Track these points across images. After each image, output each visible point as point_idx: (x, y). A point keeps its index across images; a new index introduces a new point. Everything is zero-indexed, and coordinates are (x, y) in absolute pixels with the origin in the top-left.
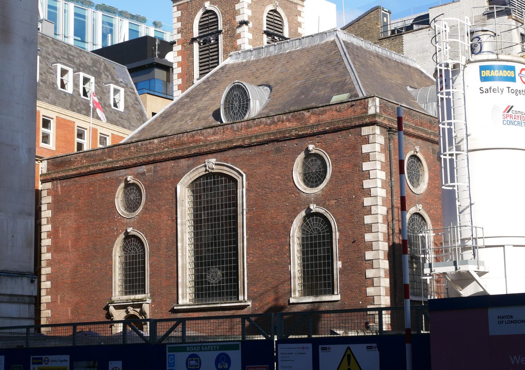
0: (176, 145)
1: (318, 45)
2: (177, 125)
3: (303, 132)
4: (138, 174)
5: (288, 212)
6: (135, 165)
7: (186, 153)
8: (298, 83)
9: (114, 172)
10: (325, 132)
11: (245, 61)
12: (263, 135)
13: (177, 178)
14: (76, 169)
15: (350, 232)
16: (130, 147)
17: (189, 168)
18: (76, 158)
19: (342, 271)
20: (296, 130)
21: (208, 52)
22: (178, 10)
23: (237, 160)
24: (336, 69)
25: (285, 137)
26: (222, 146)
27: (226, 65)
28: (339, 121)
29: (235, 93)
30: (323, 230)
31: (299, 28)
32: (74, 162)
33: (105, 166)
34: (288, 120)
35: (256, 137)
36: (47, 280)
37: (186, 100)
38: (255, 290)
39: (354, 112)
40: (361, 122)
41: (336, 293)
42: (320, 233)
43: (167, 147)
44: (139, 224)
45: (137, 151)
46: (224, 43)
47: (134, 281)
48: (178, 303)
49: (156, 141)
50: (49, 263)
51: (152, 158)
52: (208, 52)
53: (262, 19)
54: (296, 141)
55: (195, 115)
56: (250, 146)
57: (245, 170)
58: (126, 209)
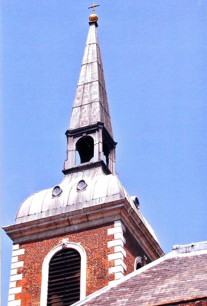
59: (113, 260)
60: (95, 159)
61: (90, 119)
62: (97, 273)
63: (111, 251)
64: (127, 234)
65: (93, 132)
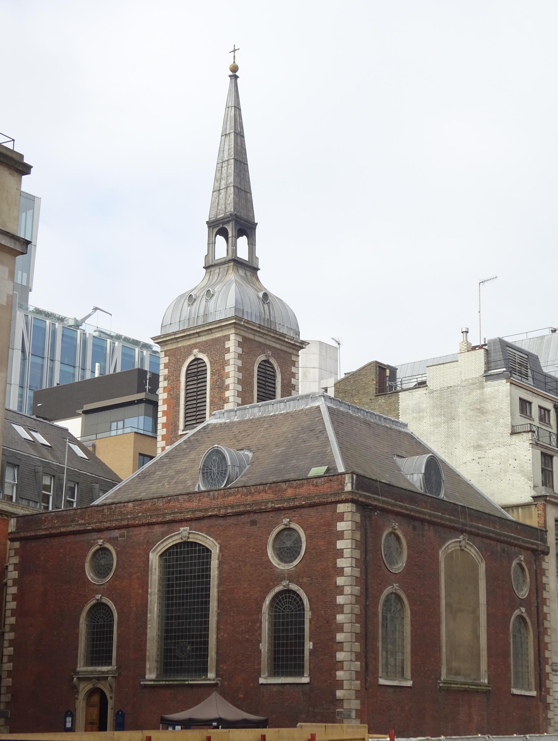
0: (150, 510)
1: (302, 410)
2: (154, 487)
3: (279, 506)
4: (110, 538)
5: (261, 587)
6: (108, 529)
7: (160, 519)
8: (279, 450)
9: (86, 535)
11: (228, 421)
12: (239, 506)
13: (150, 545)
14: (46, 529)
15: (322, 612)
16: (103, 510)
17: (163, 535)
18: (47, 517)
19: (311, 652)
21: (195, 402)
22: (166, 356)
23: (212, 530)
24: (318, 438)
25: (261, 509)
26: (198, 514)
27: (208, 425)
28: (315, 496)
29: (214, 458)
30: (296, 608)
31: (292, 379)
32: (45, 521)
33: (77, 528)
35: (232, 507)
36: (10, 646)
37: (165, 460)
38: (225, 668)
39: (331, 487)
40: (337, 499)
41: (305, 675)
43: (141, 512)
44: (110, 591)
45: (110, 514)
46: (212, 394)
48: (145, 678)
49: (130, 505)
50: (13, 628)
51: (125, 523)
52: (195, 402)
53: (253, 370)
54: (272, 514)
55: (173, 477)
56: (225, 516)
57: (220, 541)
58: (96, 575)
59: (229, 372)
61: (225, 208)
62: (218, 383)
65: (228, 222)
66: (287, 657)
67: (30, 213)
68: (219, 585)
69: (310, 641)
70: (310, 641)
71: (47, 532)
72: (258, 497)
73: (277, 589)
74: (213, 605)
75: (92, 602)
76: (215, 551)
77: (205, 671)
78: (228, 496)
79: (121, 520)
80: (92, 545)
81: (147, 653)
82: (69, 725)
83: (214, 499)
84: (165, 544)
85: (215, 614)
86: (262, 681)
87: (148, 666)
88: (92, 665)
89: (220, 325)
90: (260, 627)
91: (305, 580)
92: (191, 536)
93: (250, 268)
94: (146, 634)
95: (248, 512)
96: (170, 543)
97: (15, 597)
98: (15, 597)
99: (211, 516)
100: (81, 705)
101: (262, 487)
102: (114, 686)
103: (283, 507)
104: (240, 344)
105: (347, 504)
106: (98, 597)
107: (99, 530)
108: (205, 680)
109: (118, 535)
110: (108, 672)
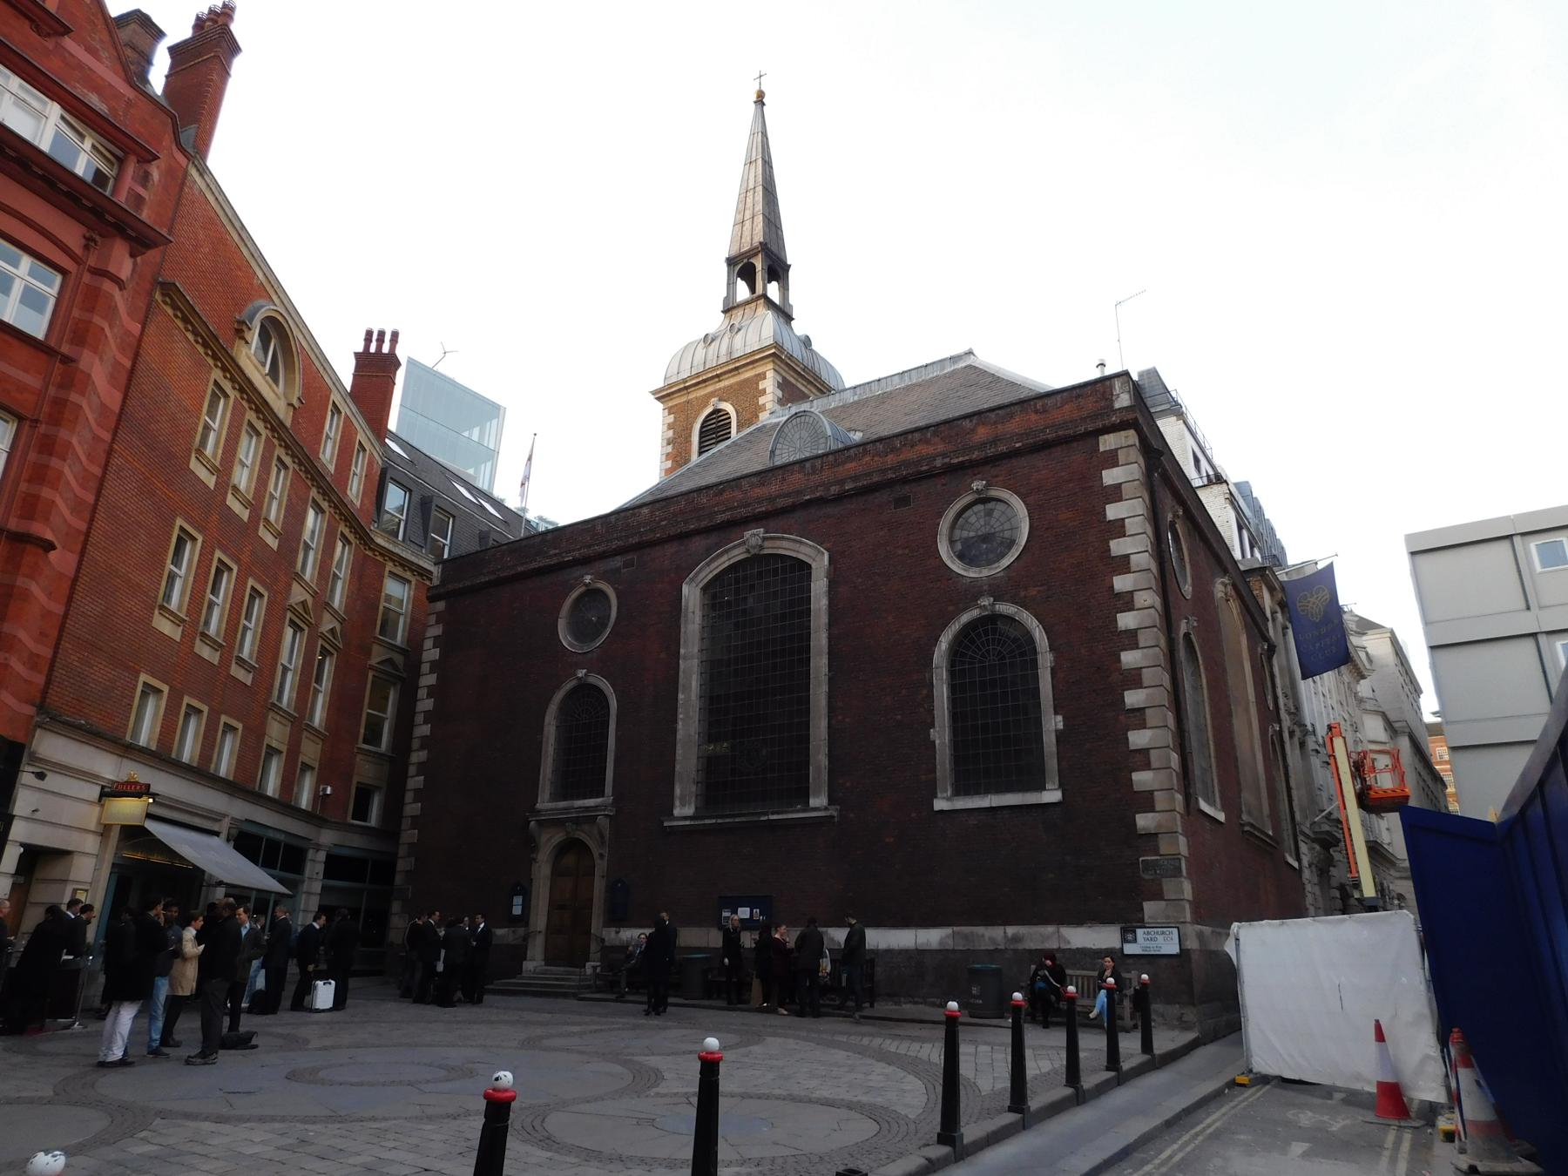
6: (602, 556)
7: (704, 524)
10: (1014, 454)
12: (870, 474)
19: (1060, 736)
20: (944, 455)
26: (780, 503)
33: (547, 562)
34: (927, 442)
35: (855, 478)
40: (1100, 424)
42: (1003, 658)
47: (580, 773)
49: (645, 510)
50: (426, 743)
56: (840, 498)
60: (759, 290)
63: (762, 408)
64: (783, 385)
65: (756, 255)
66: (995, 748)
67: (494, 422)
68: (831, 625)
69: (1056, 713)
70: (1056, 713)
71: (492, 577)
72: (910, 455)
73: (965, 618)
74: (820, 664)
75: (569, 685)
76: (820, 562)
77: (803, 795)
78: (844, 463)
79: (627, 537)
80: (572, 588)
81: (678, 767)
82: (517, 910)
83: (814, 473)
84: (713, 566)
85: (824, 680)
86: (940, 805)
87: (678, 791)
88: (565, 799)
89: (752, 360)
90: (930, 696)
91: (1033, 592)
92: (767, 544)
93: (784, 314)
94: (675, 732)
95: (890, 484)
96: (723, 563)
97: (432, 691)
98: (432, 691)
99: (809, 503)
100: (542, 870)
101: (917, 435)
102: (607, 833)
103: (970, 461)
104: (780, 386)
105: (1123, 433)
106: (581, 673)
107: (585, 562)
108: (804, 811)
109: (620, 564)
110: (596, 808)
